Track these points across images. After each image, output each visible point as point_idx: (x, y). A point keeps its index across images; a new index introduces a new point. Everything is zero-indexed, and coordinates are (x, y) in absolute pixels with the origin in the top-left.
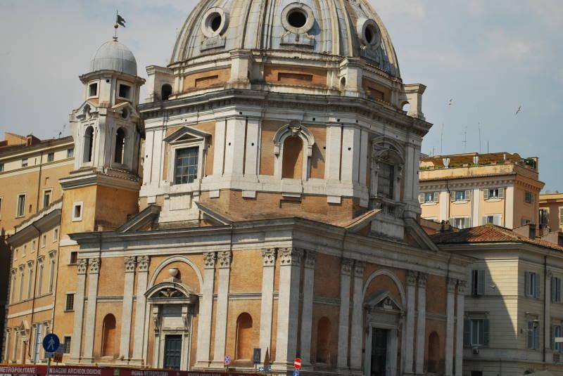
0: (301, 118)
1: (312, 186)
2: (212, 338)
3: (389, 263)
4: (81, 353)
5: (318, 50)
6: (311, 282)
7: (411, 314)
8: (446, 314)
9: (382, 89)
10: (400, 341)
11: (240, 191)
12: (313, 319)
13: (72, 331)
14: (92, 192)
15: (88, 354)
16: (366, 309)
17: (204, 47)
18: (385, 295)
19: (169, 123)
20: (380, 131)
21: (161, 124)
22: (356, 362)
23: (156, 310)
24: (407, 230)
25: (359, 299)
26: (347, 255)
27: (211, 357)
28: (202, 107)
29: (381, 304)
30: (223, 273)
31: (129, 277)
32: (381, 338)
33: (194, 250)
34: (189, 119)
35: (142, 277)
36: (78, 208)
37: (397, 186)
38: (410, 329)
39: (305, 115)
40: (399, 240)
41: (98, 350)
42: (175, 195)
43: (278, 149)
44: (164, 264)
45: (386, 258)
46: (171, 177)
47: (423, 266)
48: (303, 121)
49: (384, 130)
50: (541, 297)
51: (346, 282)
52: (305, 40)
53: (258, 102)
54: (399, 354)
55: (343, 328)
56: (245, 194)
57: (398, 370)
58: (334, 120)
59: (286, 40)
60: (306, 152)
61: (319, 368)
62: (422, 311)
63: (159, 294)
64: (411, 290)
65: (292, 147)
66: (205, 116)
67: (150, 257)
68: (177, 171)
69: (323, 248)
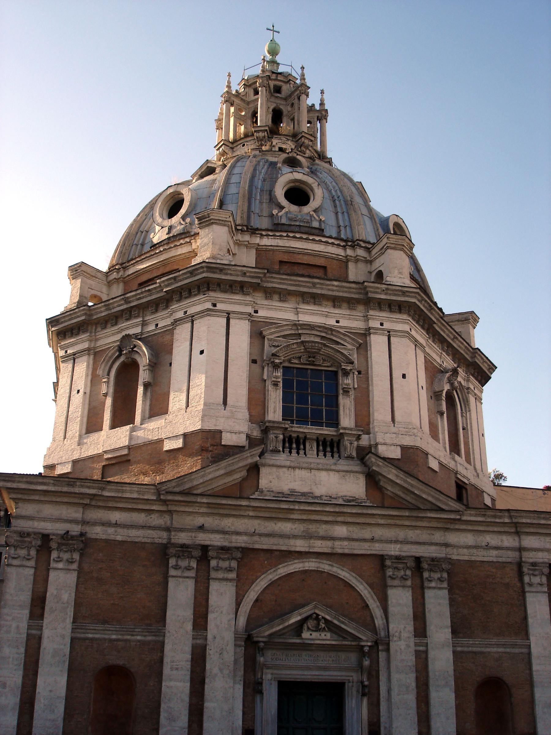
1: (152, 430)
3: (320, 546)
6: (68, 596)
7: (403, 648)
8: (527, 636)
9: (321, 262)
10: (375, 706)
12: (74, 670)
18: (306, 611)
24: (373, 479)
26: (183, 538)
39: (144, 324)
40: (351, 502)
45: (308, 536)
47: (432, 544)
48: (142, 333)
49: (297, 314)
58: (180, 314)
60: (144, 376)
65: (127, 373)
69: (111, 530)
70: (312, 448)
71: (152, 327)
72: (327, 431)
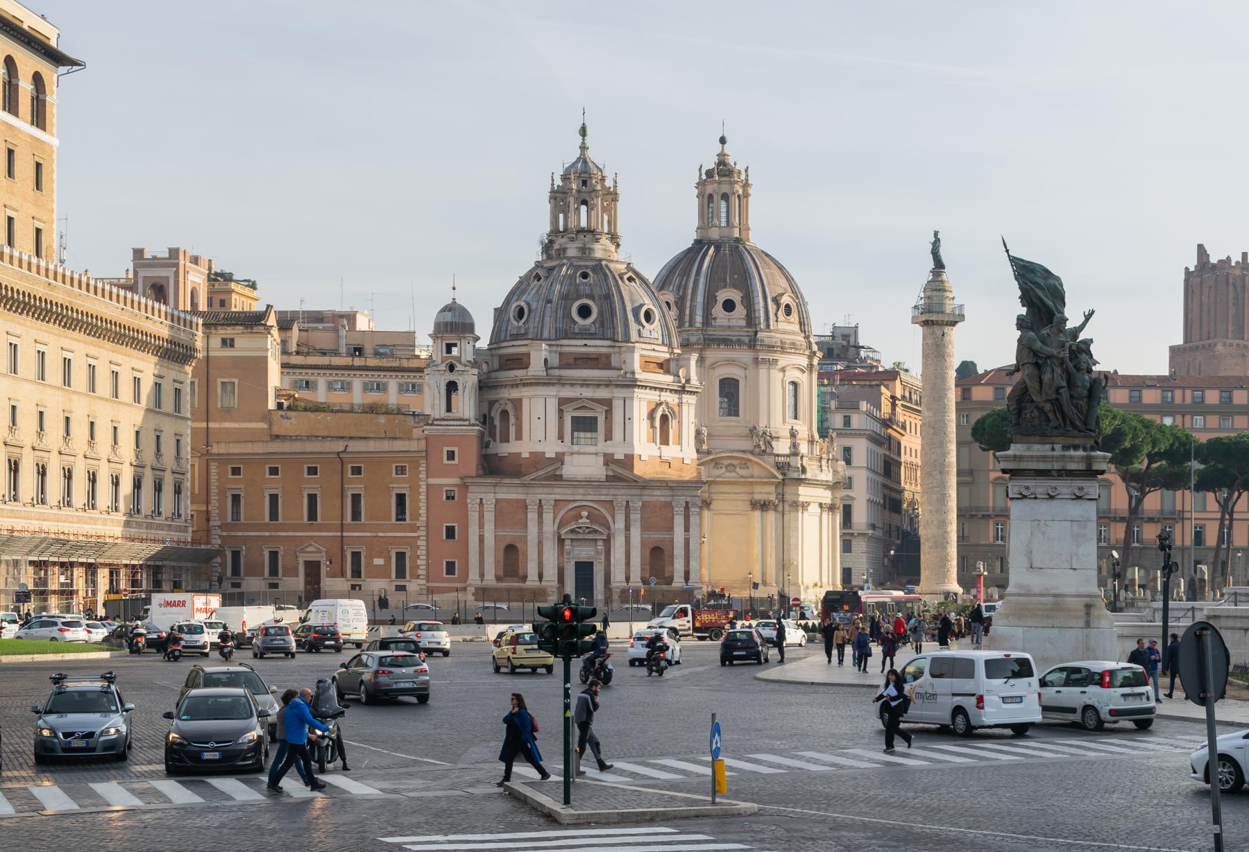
2: (628, 564)
4: (482, 575)
17: (577, 331)
21: (554, 393)
27: (628, 579)
28: (598, 386)
30: (636, 517)
33: (603, 498)
34: (587, 393)
35: (548, 517)
41: (501, 573)
42: (579, 453)
43: (657, 423)
44: (571, 506)
52: (654, 335)
63: (572, 531)
66: (603, 393)
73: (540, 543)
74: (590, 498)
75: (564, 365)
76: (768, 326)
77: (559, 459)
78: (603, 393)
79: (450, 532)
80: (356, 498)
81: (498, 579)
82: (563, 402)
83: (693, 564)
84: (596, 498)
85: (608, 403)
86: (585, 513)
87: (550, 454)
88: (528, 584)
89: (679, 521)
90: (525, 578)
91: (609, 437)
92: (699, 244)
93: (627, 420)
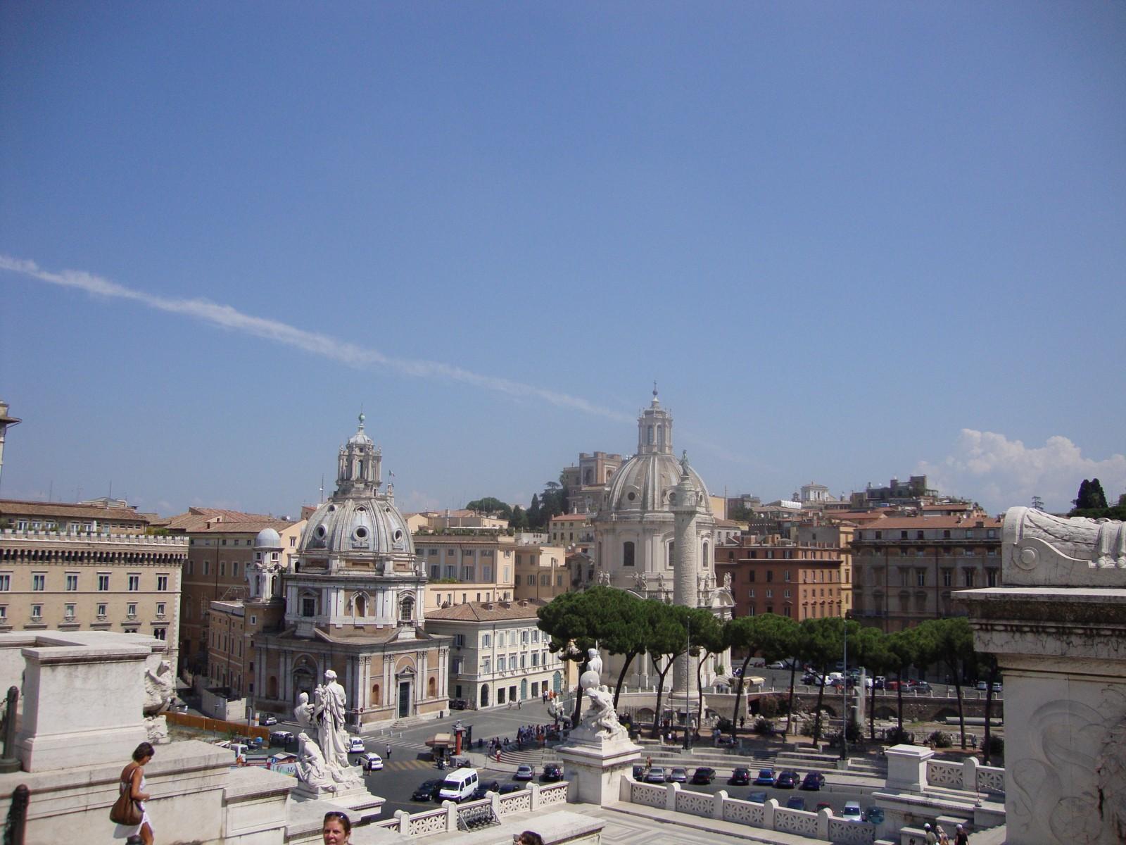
0: (363, 587)
5: (371, 549)
11: (335, 625)
13: (254, 681)
14: (261, 614)
15: (263, 695)
16: (397, 676)
19: (300, 585)
20: (402, 587)
22: (392, 702)
23: (296, 678)
25: (393, 673)
29: (404, 672)
31: (282, 659)
32: (404, 688)
34: (310, 584)
35: (289, 661)
36: (254, 618)
37: (412, 611)
38: (420, 680)
39: (365, 586)
43: (353, 604)
44: (300, 655)
46: (301, 612)
50: (492, 646)
51: (386, 666)
53: (342, 581)
54: (414, 692)
55: (386, 687)
56: (337, 626)
57: (414, 700)
59: (356, 545)
61: (374, 708)
62: (426, 669)
63: (298, 671)
64: (420, 661)
65: (360, 602)
66: (317, 585)
67: (293, 651)
68: (305, 610)
70: (406, 625)
71: (368, 588)
72: (409, 621)
73: (285, 677)
74: (308, 650)
75: (307, 566)
76: (654, 508)
77: (295, 626)
78: (317, 585)
79: (252, 665)
80: (233, 640)
81: (267, 698)
82: (300, 589)
83: (355, 696)
84: (310, 651)
85: (319, 591)
86: (304, 661)
87: (292, 623)
88: (278, 702)
89: (349, 668)
90: (277, 699)
91: (320, 613)
92: (635, 456)
93: (329, 601)
